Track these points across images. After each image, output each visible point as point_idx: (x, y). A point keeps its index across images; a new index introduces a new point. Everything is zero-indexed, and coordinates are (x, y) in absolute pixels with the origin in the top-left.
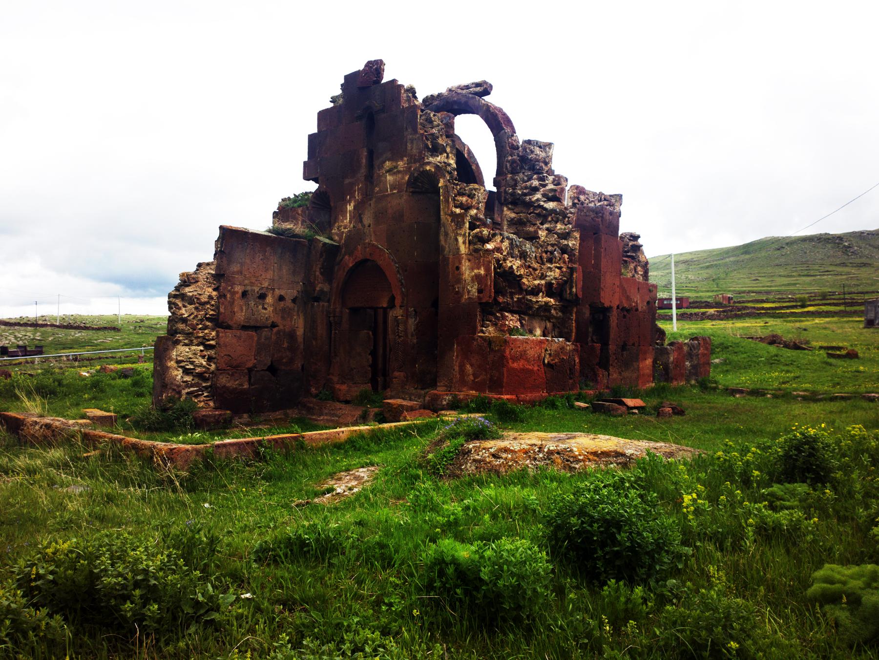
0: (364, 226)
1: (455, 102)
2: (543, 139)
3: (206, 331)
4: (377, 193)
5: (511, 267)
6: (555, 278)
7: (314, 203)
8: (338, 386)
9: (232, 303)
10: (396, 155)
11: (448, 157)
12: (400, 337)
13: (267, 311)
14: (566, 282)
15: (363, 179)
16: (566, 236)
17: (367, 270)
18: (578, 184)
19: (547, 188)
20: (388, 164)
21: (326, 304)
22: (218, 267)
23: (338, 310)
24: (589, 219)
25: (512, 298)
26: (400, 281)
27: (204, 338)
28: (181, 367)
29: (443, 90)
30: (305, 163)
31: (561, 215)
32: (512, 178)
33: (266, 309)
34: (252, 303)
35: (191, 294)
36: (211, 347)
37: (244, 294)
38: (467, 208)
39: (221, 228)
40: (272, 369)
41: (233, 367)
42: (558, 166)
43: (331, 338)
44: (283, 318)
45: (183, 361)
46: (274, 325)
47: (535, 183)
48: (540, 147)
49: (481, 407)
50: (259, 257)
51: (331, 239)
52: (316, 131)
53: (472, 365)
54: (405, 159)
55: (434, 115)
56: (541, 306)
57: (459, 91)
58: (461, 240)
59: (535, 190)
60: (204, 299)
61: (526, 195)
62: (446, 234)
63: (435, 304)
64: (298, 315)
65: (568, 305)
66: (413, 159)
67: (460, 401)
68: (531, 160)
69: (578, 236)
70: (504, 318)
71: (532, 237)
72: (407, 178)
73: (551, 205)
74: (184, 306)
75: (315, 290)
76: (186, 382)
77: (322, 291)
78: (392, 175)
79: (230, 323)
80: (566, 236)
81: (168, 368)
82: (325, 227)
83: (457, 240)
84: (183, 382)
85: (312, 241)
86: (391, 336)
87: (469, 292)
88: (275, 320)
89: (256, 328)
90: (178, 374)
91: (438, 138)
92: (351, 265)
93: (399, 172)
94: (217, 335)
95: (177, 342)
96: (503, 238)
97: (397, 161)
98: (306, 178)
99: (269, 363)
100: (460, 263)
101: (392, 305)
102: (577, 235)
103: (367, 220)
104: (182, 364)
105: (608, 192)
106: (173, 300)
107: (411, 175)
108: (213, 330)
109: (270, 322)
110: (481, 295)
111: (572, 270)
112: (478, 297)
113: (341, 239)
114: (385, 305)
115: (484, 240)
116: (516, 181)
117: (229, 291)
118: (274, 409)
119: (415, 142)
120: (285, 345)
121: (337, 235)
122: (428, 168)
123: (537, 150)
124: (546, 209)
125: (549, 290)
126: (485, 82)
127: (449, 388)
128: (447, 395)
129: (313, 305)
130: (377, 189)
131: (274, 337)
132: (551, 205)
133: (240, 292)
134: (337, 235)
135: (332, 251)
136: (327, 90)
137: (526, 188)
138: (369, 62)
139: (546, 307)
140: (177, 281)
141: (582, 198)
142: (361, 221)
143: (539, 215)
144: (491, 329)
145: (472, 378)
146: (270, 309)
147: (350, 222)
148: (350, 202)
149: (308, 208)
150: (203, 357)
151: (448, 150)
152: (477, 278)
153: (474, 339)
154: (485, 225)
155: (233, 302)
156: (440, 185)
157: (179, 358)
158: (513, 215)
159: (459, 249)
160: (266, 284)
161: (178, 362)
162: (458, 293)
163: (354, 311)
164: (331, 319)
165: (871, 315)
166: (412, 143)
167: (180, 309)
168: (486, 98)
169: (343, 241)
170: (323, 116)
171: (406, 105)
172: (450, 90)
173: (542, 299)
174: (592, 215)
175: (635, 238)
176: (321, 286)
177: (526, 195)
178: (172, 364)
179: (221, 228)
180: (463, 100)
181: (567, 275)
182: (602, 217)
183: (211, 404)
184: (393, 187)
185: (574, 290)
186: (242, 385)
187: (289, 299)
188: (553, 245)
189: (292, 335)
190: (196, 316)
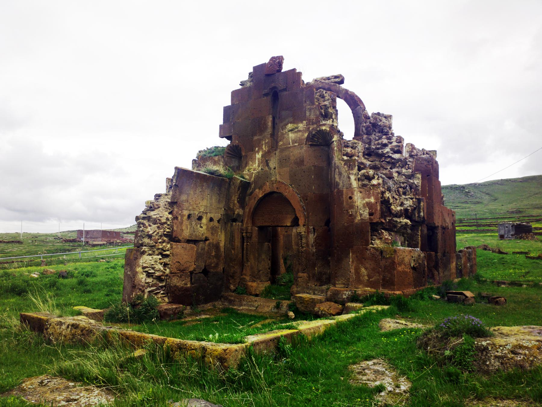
0: (270, 169)
2: (386, 113)
3: (164, 244)
4: (281, 146)
6: (410, 206)
7: (228, 153)
8: (250, 284)
9: (181, 223)
10: (297, 119)
11: (333, 121)
12: (303, 247)
13: (202, 230)
14: (415, 209)
15: (269, 136)
16: (411, 176)
17: (274, 199)
18: (413, 143)
20: (290, 126)
21: (240, 224)
23: (250, 228)
24: (423, 166)
25: (385, 220)
27: (162, 249)
28: (146, 272)
30: (221, 126)
31: (404, 163)
32: (367, 138)
33: (201, 227)
34: (194, 223)
35: (155, 217)
36: (167, 256)
37: (189, 216)
39: (176, 168)
40: (205, 272)
41: (181, 271)
42: (397, 130)
44: (212, 233)
45: (147, 267)
46: (207, 239)
47: (385, 141)
48: (385, 117)
49: (381, 300)
51: (244, 178)
52: (230, 104)
53: (366, 269)
54: (305, 122)
55: (326, 93)
56: (402, 226)
57: (323, 81)
58: (353, 177)
59: (385, 145)
60: (164, 220)
61: (378, 149)
62: (340, 174)
64: (221, 232)
66: (310, 122)
67: (359, 295)
68: (380, 126)
69: (420, 177)
72: (306, 135)
73: (396, 156)
74: (150, 226)
75: (234, 214)
76: (148, 283)
77: (238, 214)
78: (294, 133)
79: (180, 238)
81: (137, 272)
82: (239, 168)
83: (349, 178)
84: (146, 283)
85: (231, 179)
87: (361, 215)
88: (207, 235)
89: (195, 242)
90: (142, 277)
92: (261, 196)
93: (300, 131)
94: (172, 247)
95: (143, 253)
96: (378, 177)
97: (297, 123)
100: (353, 194)
102: (419, 176)
104: (147, 269)
105: (428, 149)
107: (310, 133)
108: (168, 243)
109: (204, 237)
110: (372, 217)
112: (370, 218)
113: (251, 178)
114: (289, 224)
115: (370, 178)
116: (370, 139)
117: (180, 214)
118: (206, 302)
119: (312, 111)
120: (213, 254)
122: (324, 128)
123: (384, 120)
124: (393, 159)
125: (406, 213)
126: (341, 76)
127: (347, 285)
128: (347, 291)
129: (232, 225)
130: (281, 143)
131: (206, 248)
132: (396, 156)
133: (187, 215)
134: (248, 175)
135: (245, 186)
137: (378, 144)
138: (273, 58)
140: (144, 208)
142: (268, 165)
143: (388, 163)
144: (378, 242)
145: (366, 278)
146: (204, 227)
147: (259, 166)
148: (258, 152)
150: (161, 264)
152: (369, 205)
153: (367, 249)
155: (182, 223)
156: (334, 139)
157: (145, 265)
159: (351, 184)
160: (202, 210)
162: (351, 215)
163: (261, 228)
164: (244, 234)
165: (502, 232)
167: (147, 227)
168: (342, 86)
169: (253, 179)
170: (235, 94)
172: (316, 80)
174: (425, 163)
176: (238, 211)
177: (378, 149)
178: (139, 269)
179: (176, 168)
182: (432, 165)
183: (166, 299)
184: (294, 142)
185: (422, 214)
186: (186, 284)
187: (216, 219)
188: (403, 183)
189: (217, 246)
190: (158, 233)
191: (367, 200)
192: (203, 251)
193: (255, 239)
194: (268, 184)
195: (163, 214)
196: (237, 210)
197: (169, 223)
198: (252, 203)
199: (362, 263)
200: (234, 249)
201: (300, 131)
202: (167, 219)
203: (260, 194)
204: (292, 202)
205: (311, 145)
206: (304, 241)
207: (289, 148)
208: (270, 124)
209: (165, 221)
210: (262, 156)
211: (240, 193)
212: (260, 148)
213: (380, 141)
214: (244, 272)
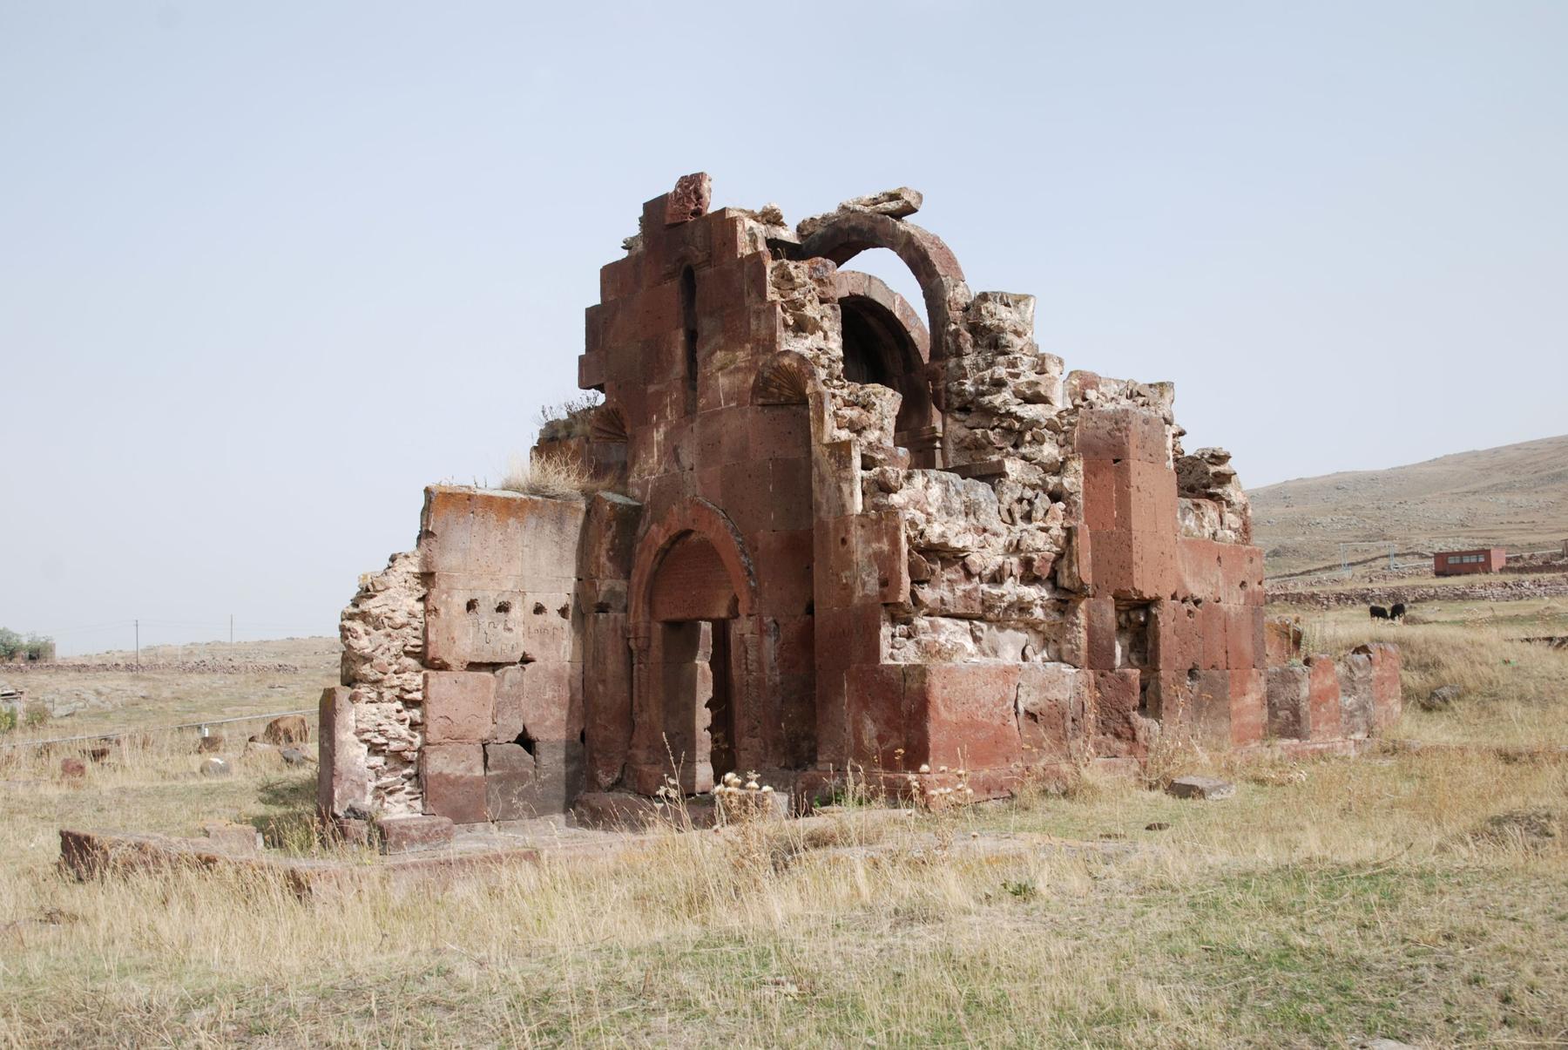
0: (682, 469)
1: (853, 229)
3: (405, 676)
5: (943, 535)
8: (646, 769)
10: (734, 339)
11: (826, 337)
15: (679, 384)
16: (1058, 469)
19: (1023, 379)
21: (621, 616)
22: (425, 561)
24: (1101, 432)
26: (746, 568)
28: (366, 741)
29: (832, 209)
30: (581, 358)
37: (471, 605)
38: (858, 429)
43: (631, 679)
44: (542, 644)
46: (526, 660)
47: (1001, 372)
50: (496, 536)
52: (598, 302)
54: (748, 346)
56: (1011, 605)
59: (999, 384)
60: (400, 618)
61: (983, 394)
62: (822, 480)
63: (810, 610)
65: (1066, 598)
70: (935, 628)
71: (993, 476)
72: (751, 380)
73: (1029, 411)
79: (447, 659)
80: (1058, 469)
83: (840, 489)
86: (735, 672)
89: (494, 666)
91: (804, 305)
92: (661, 542)
93: (738, 369)
97: (734, 351)
98: (584, 385)
99: (520, 730)
100: (847, 531)
101: (734, 613)
102: (1077, 465)
103: (688, 457)
104: (367, 736)
106: (348, 624)
107: (760, 375)
110: (885, 590)
111: (1070, 533)
112: (881, 593)
113: (644, 493)
121: (638, 486)
122: (786, 361)
124: (1020, 419)
129: (596, 619)
130: (702, 402)
134: (638, 486)
136: (614, 232)
139: (1023, 607)
140: (354, 591)
141: (1092, 395)
142: (678, 460)
147: (659, 463)
148: (657, 426)
149: (587, 440)
151: (826, 324)
154: (894, 460)
157: (361, 726)
158: (963, 432)
160: (509, 586)
161: (359, 733)
162: (846, 587)
164: (632, 643)
166: (758, 318)
169: (648, 498)
170: (610, 274)
171: (748, 251)
172: (844, 208)
173: (1012, 589)
175: (1219, 459)
180: (866, 225)
181: (1061, 541)
186: (470, 769)
187: (552, 607)
188: (1033, 487)
191: (875, 546)
192: (515, 689)
193: (657, 652)
194: (675, 508)
195: (401, 602)
196: (608, 582)
197: (416, 624)
198: (645, 561)
199: (866, 707)
200: (604, 682)
201: (738, 369)
202: (412, 615)
203: (658, 536)
204: (723, 555)
205: (763, 405)
206: (752, 656)
207: (720, 413)
208: (679, 352)
209: (405, 620)
210: (666, 434)
211: (614, 537)
212: (662, 416)
213: (987, 374)
214: (635, 740)
